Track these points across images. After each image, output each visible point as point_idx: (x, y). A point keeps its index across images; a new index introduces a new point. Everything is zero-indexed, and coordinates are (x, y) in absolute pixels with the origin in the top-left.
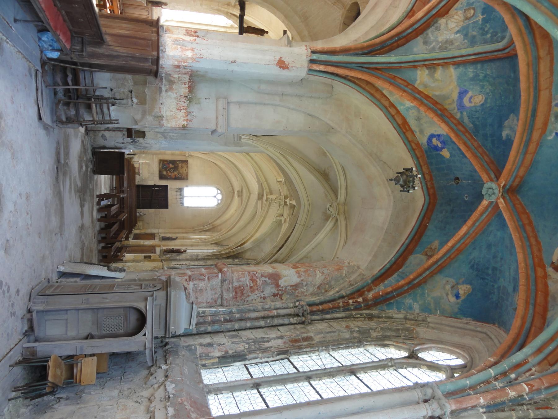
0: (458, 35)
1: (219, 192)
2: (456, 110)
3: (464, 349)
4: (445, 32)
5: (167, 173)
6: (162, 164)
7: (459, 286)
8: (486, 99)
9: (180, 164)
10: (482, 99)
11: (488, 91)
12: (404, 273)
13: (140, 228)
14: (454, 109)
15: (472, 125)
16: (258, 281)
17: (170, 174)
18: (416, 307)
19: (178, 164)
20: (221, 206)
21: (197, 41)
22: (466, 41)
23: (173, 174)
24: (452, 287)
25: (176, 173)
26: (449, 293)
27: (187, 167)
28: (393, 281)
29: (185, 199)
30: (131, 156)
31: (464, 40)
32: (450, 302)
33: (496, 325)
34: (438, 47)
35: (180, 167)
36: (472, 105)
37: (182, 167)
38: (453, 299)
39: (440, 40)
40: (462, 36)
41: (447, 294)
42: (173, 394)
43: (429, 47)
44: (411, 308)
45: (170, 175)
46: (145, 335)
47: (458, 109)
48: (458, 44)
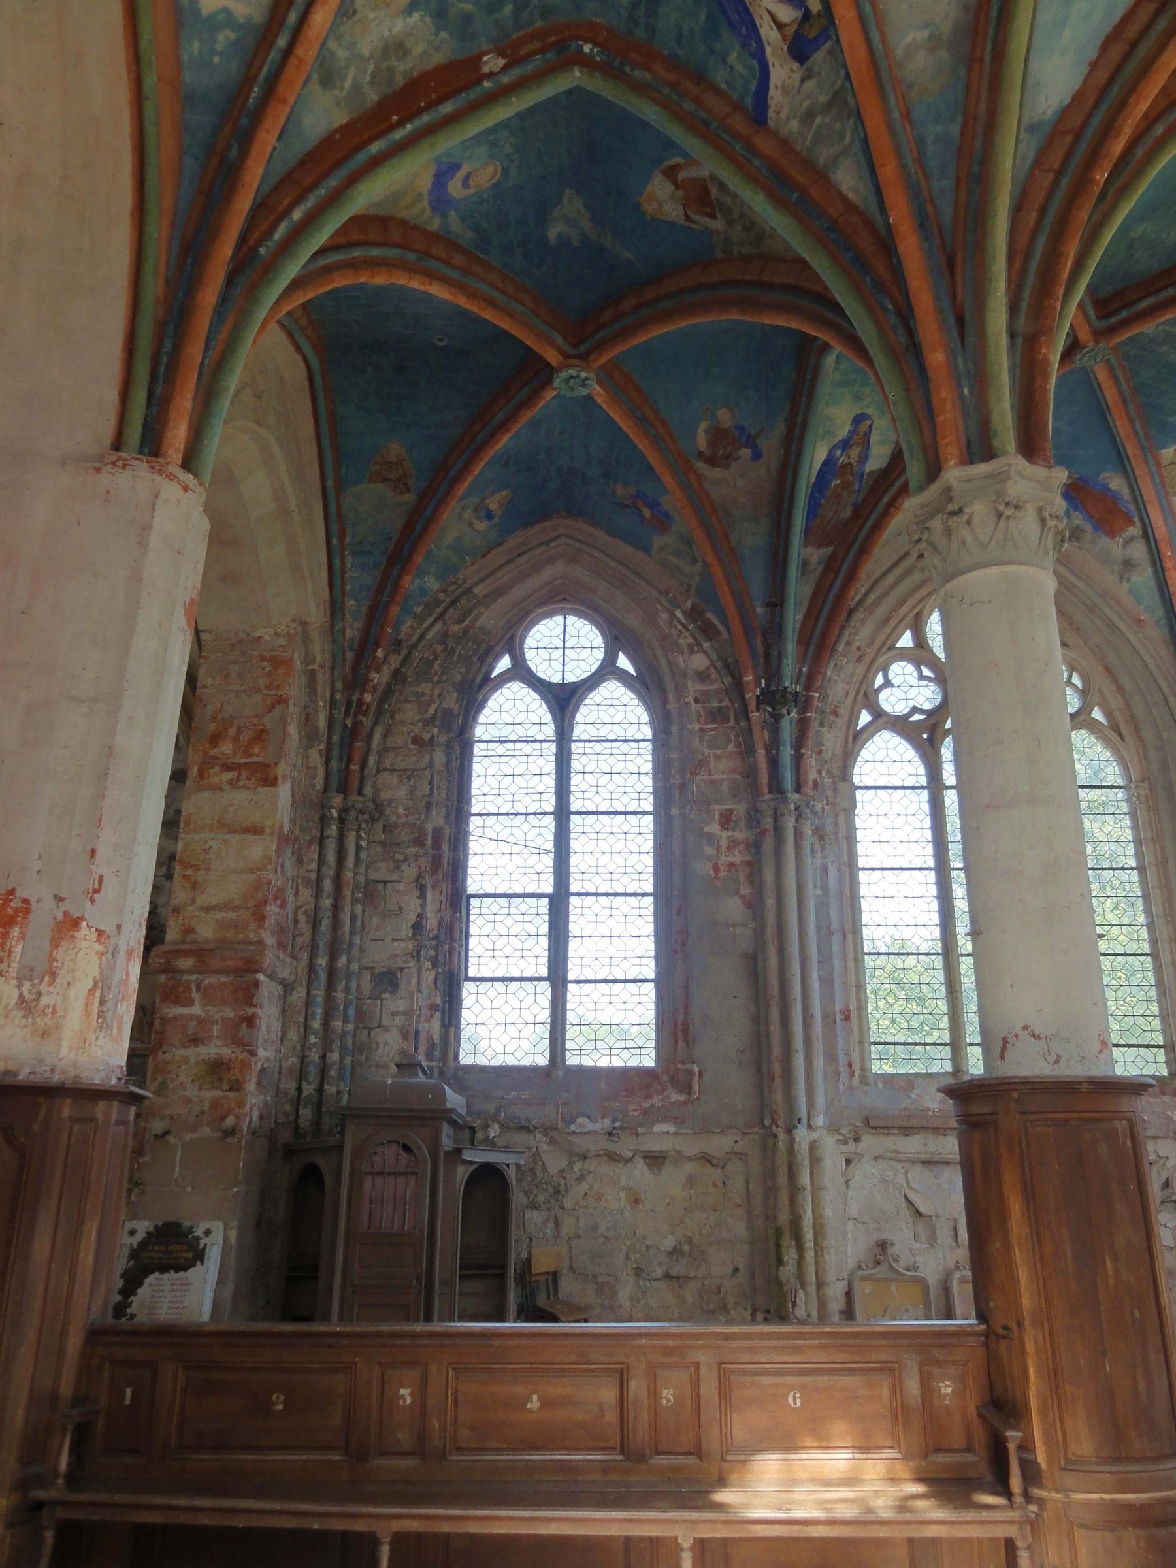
0: (416, 16)
2: (428, 212)
3: (562, 596)
4: (372, 15)
7: (487, 502)
8: (505, 171)
10: (496, 171)
11: (508, 149)
12: (361, 542)
14: (423, 212)
15: (471, 234)
16: (279, 883)
18: (432, 584)
21: (110, 929)
22: (443, 35)
24: (476, 510)
26: (473, 520)
28: (357, 574)
31: (437, 33)
32: (480, 532)
33: (563, 514)
34: (368, 78)
36: (472, 191)
38: (482, 526)
39: (366, 54)
40: (428, 19)
41: (471, 525)
42: (614, 1121)
43: (342, 89)
44: (424, 592)
46: (508, 1165)
47: (434, 210)
48: (421, 48)
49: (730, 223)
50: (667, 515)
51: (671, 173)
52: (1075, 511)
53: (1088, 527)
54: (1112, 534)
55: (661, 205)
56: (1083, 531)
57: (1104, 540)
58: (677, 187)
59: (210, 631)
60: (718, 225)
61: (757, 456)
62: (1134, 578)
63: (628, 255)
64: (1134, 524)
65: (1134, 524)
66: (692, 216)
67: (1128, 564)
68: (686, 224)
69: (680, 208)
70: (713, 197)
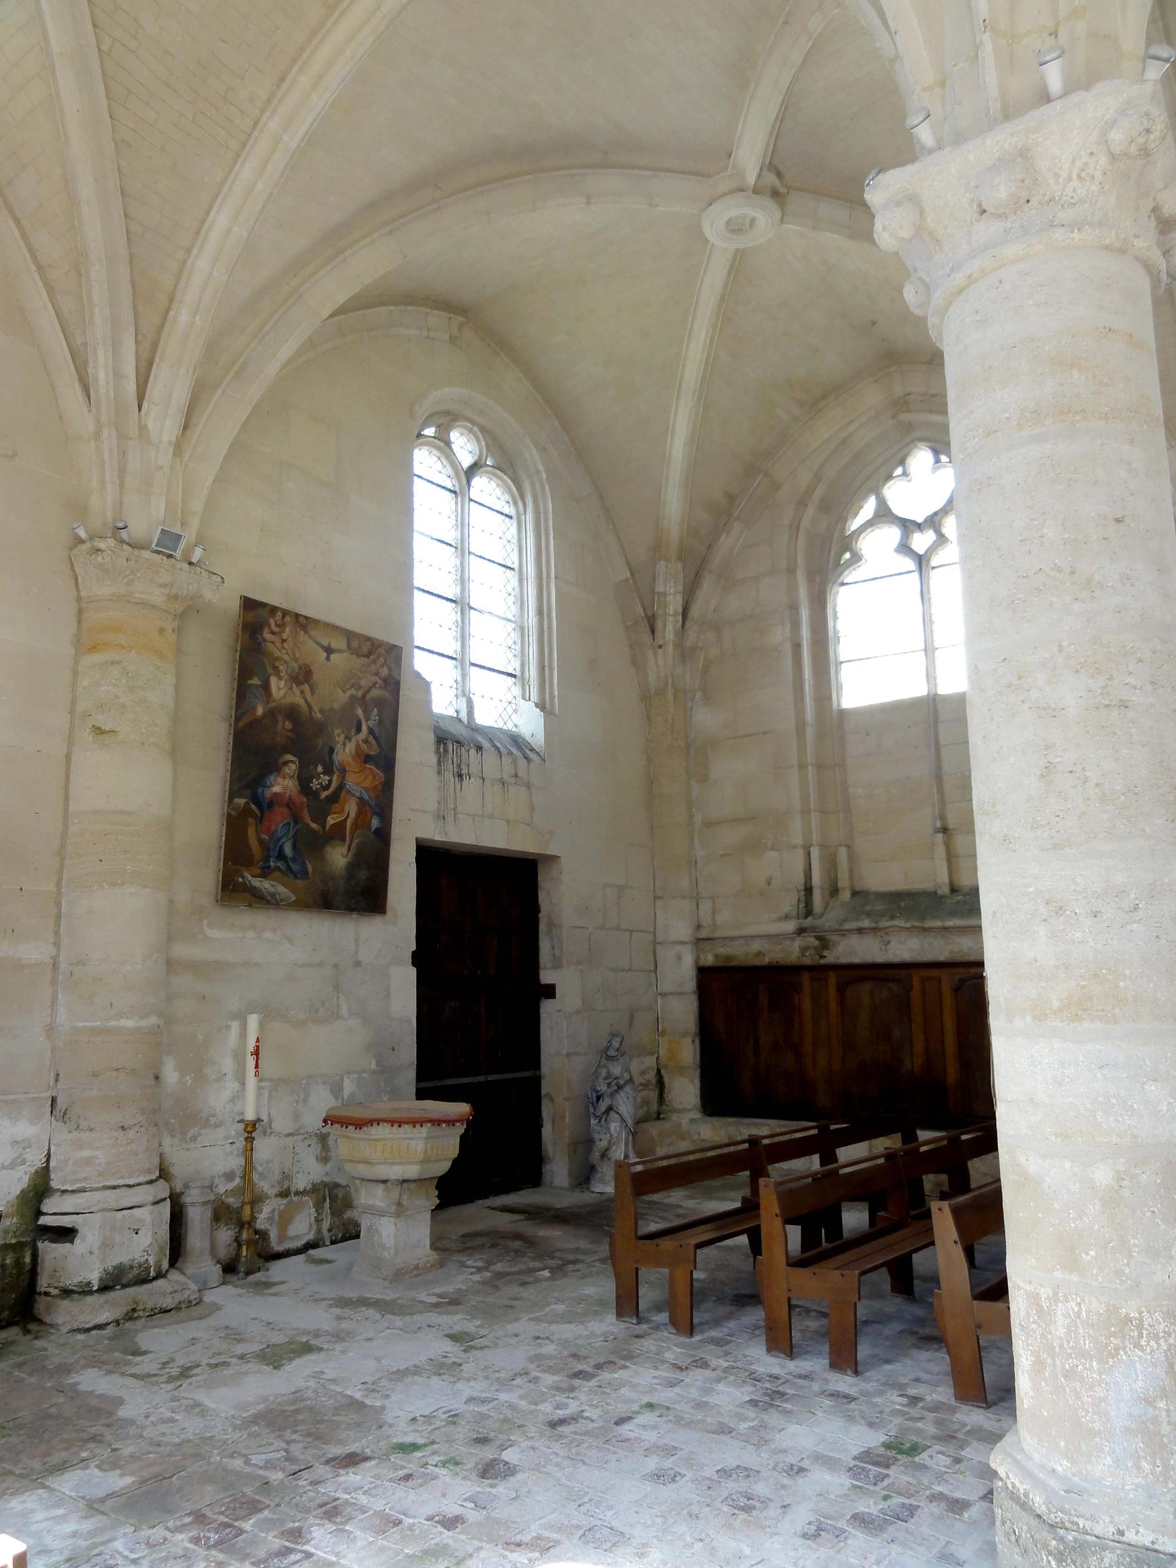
1: (430, 431)
5: (337, 834)
6: (265, 873)
9: (278, 688)
13: (651, 1076)
17: (351, 807)
19: (272, 714)
20: (533, 457)
23: (352, 781)
25: (345, 753)
27: (303, 623)
29: (485, 717)
30: (197, 1217)
35: (296, 698)
37: (303, 676)
45: (362, 802)
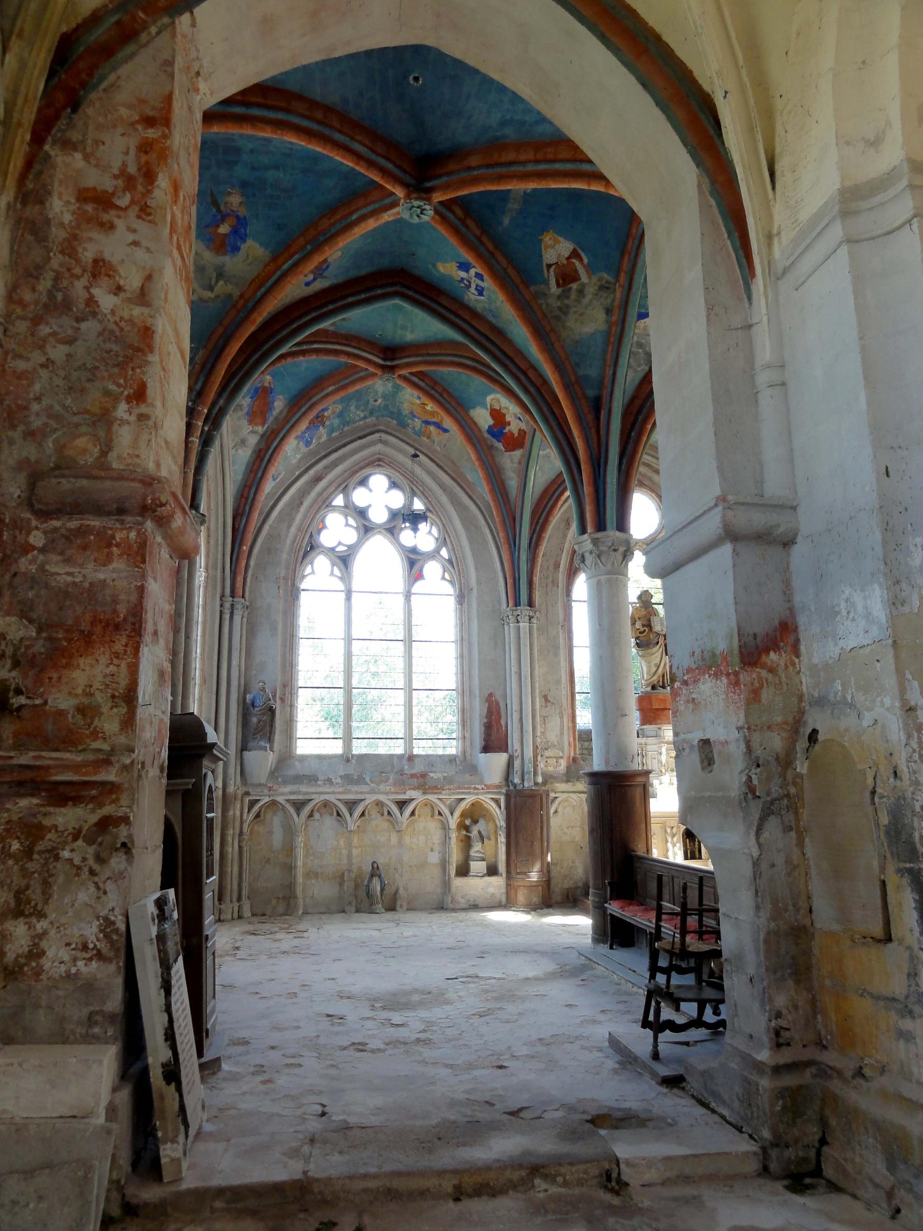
49: (559, 297)
50: (236, 249)
51: (575, 254)
52: (251, 398)
53: (245, 410)
54: (251, 422)
55: (553, 247)
56: (242, 410)
57: (245, 422)
58: (568, 258)
59: (193, 25)
60: (554, 289)
61: (307, 284)
62: (240, 451)
63: (506, 221)
64: (263, 426)
65: (263, 426)
66: (552, 269)
67: (243, 442)
68: (544, 265)
69: (555, 261)
70: (571, 285)
